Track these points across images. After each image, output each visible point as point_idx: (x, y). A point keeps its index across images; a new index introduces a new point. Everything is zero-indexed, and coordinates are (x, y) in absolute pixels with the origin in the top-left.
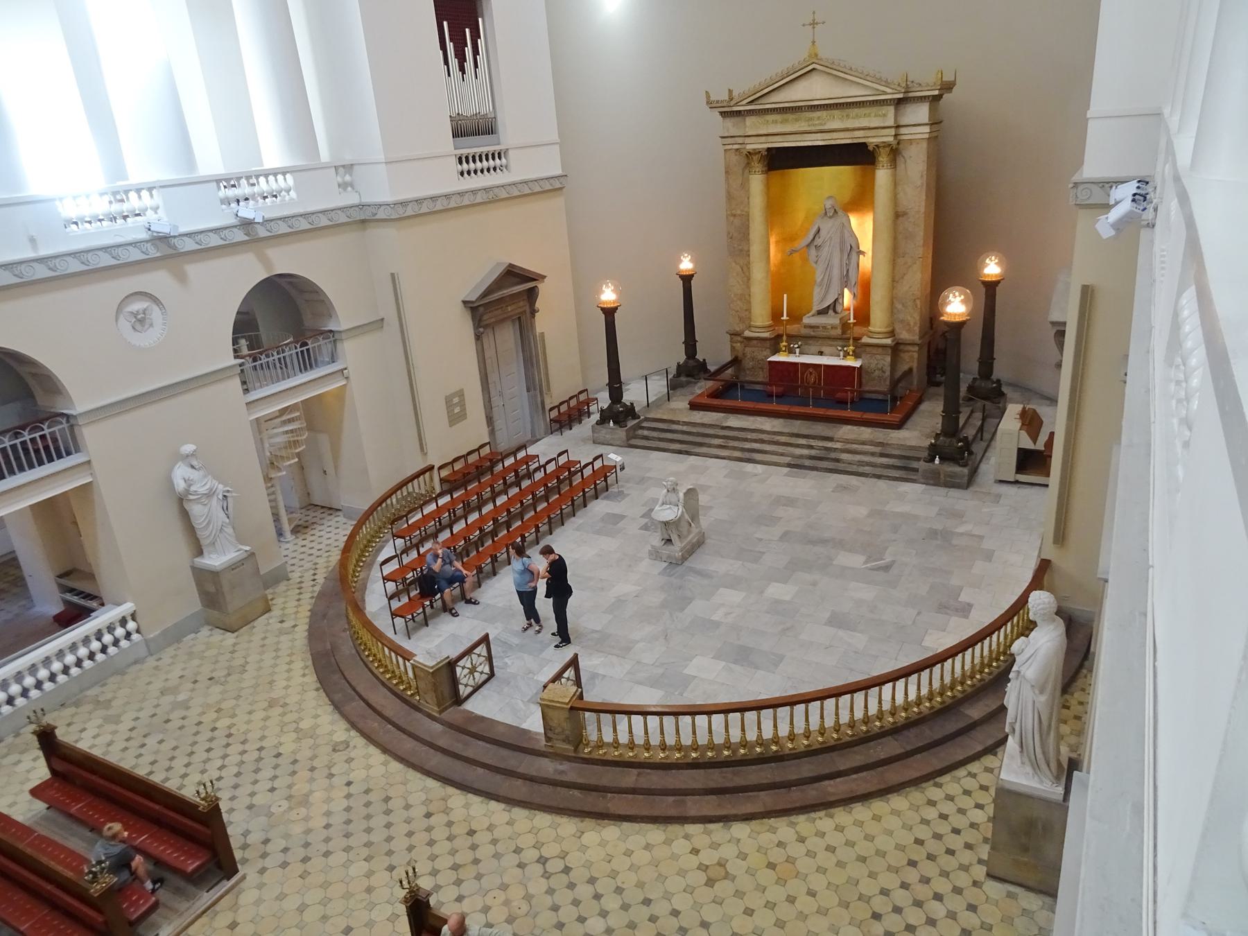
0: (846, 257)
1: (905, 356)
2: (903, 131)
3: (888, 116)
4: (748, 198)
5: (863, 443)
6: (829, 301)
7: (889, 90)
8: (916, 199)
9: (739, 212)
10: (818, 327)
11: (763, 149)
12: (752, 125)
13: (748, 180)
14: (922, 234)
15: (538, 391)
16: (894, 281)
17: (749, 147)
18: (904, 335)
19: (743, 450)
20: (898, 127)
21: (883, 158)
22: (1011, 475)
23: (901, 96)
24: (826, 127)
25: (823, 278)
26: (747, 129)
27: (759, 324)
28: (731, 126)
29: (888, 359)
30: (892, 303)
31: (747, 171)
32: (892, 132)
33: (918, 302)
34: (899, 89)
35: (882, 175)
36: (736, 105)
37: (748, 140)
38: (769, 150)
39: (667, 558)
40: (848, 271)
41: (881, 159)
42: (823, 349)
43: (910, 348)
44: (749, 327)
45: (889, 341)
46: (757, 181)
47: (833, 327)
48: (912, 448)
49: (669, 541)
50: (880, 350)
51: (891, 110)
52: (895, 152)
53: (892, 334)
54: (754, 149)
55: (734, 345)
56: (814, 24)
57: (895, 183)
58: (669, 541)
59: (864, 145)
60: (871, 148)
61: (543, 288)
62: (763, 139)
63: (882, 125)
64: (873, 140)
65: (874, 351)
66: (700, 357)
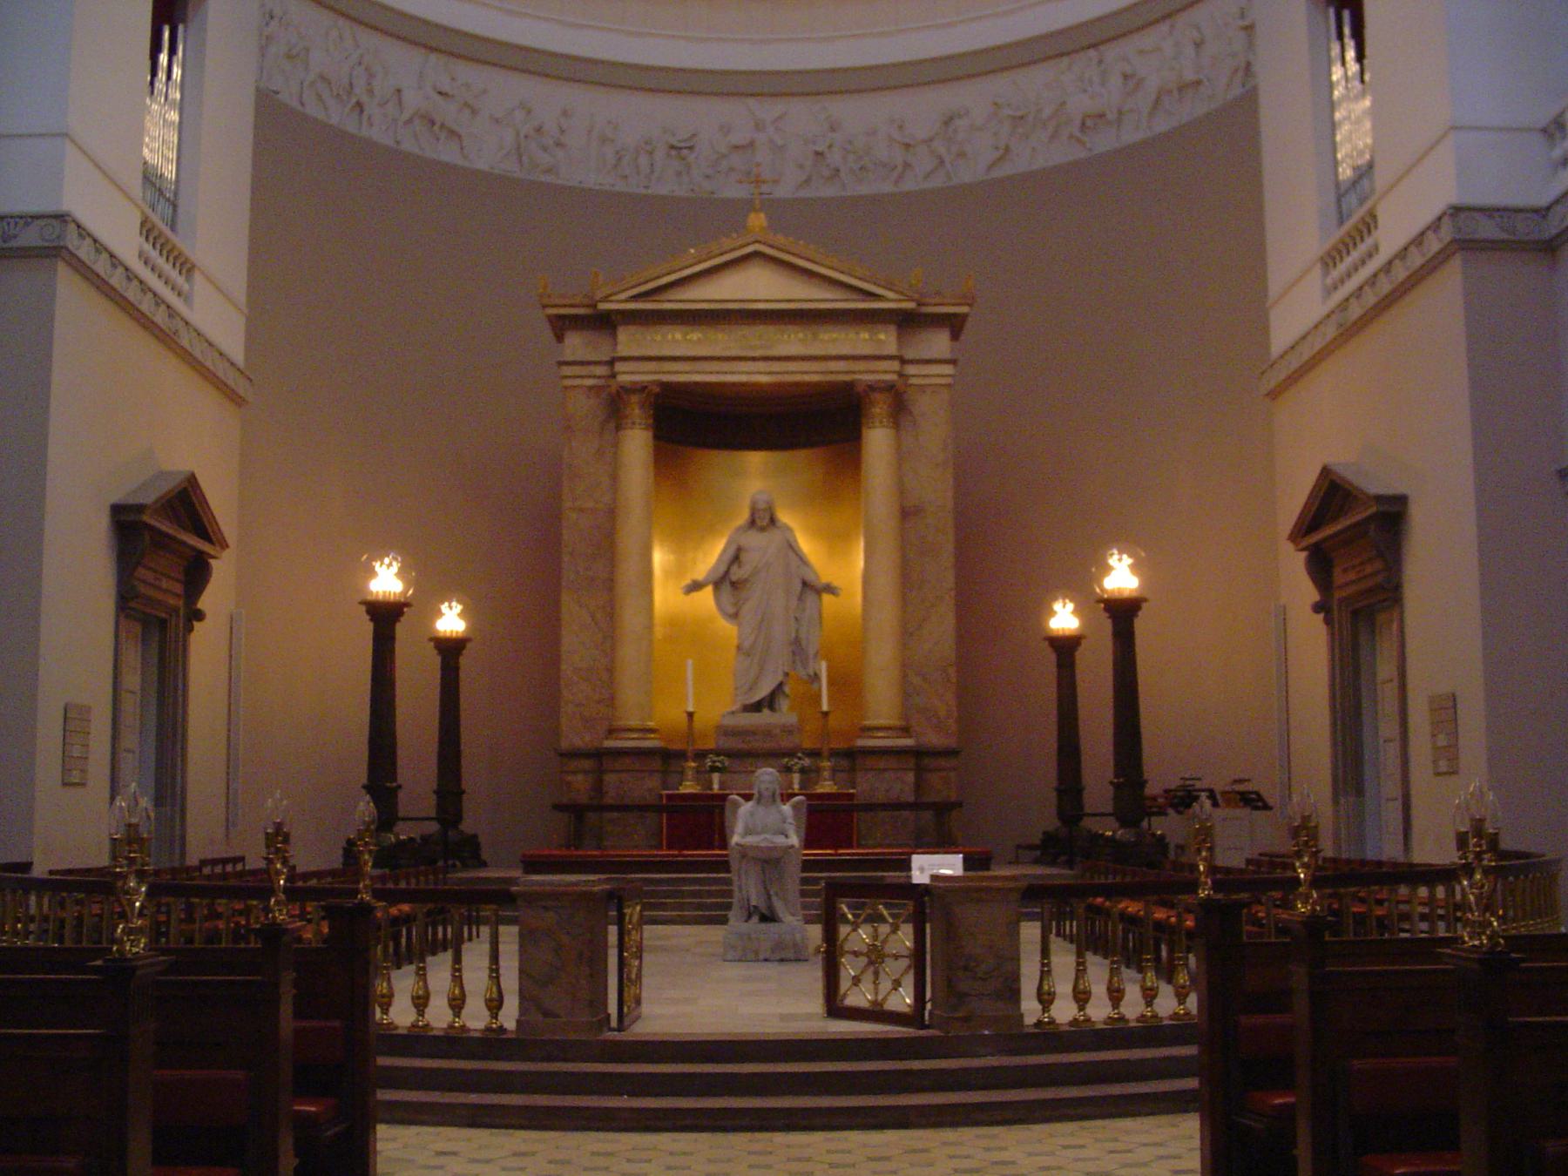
0: (794, 602)
1: (934, 779)
2: (911, 370)
3: (886, 339)
4: (615, 479)
6: (763, 692)
7: (890, 295)
8: (936, 490)
9: (591, 504)
10: (754, 733)
11: (648, 382)
12: (629, 341)
13: (616, 445)
14: (950, 547)
15: (177, 809)
16: (907, 633)
17: (624, 379)
18: (934, 739)
19: (700, 907)
20: (904, 361)
21: (879, 408)
23: (910, 305)
25: (755, 642)
26: (619, 347)
27: (634, 722)
28: (576, 344)
29: (910, 777)
30: (905, 676)
31: (612, 425)
32: (896, 365)
33: (952, 671)
34: (911, 294)
35: (877, 440)
36: (606, 299)
37: (619, 367)
38: (665, 386)
39: (773, 951)
40: (797, 631)
41: (876, 410)
43: (943, 762)
44: (611, 732)
46: (637, 444)
47: (788, 730)
51: (892, 329)
52: (899, 402)
53: (905, 731)
54: (635, 383)
55: (570, 778)
56: (757, 182)
57: (901, 456)
59: (850, 386)
60: (860, 389)
61: (222, 569)
62: (652, 366)
63: (877, 353)
64: (865, 375)
66: (467, 826)
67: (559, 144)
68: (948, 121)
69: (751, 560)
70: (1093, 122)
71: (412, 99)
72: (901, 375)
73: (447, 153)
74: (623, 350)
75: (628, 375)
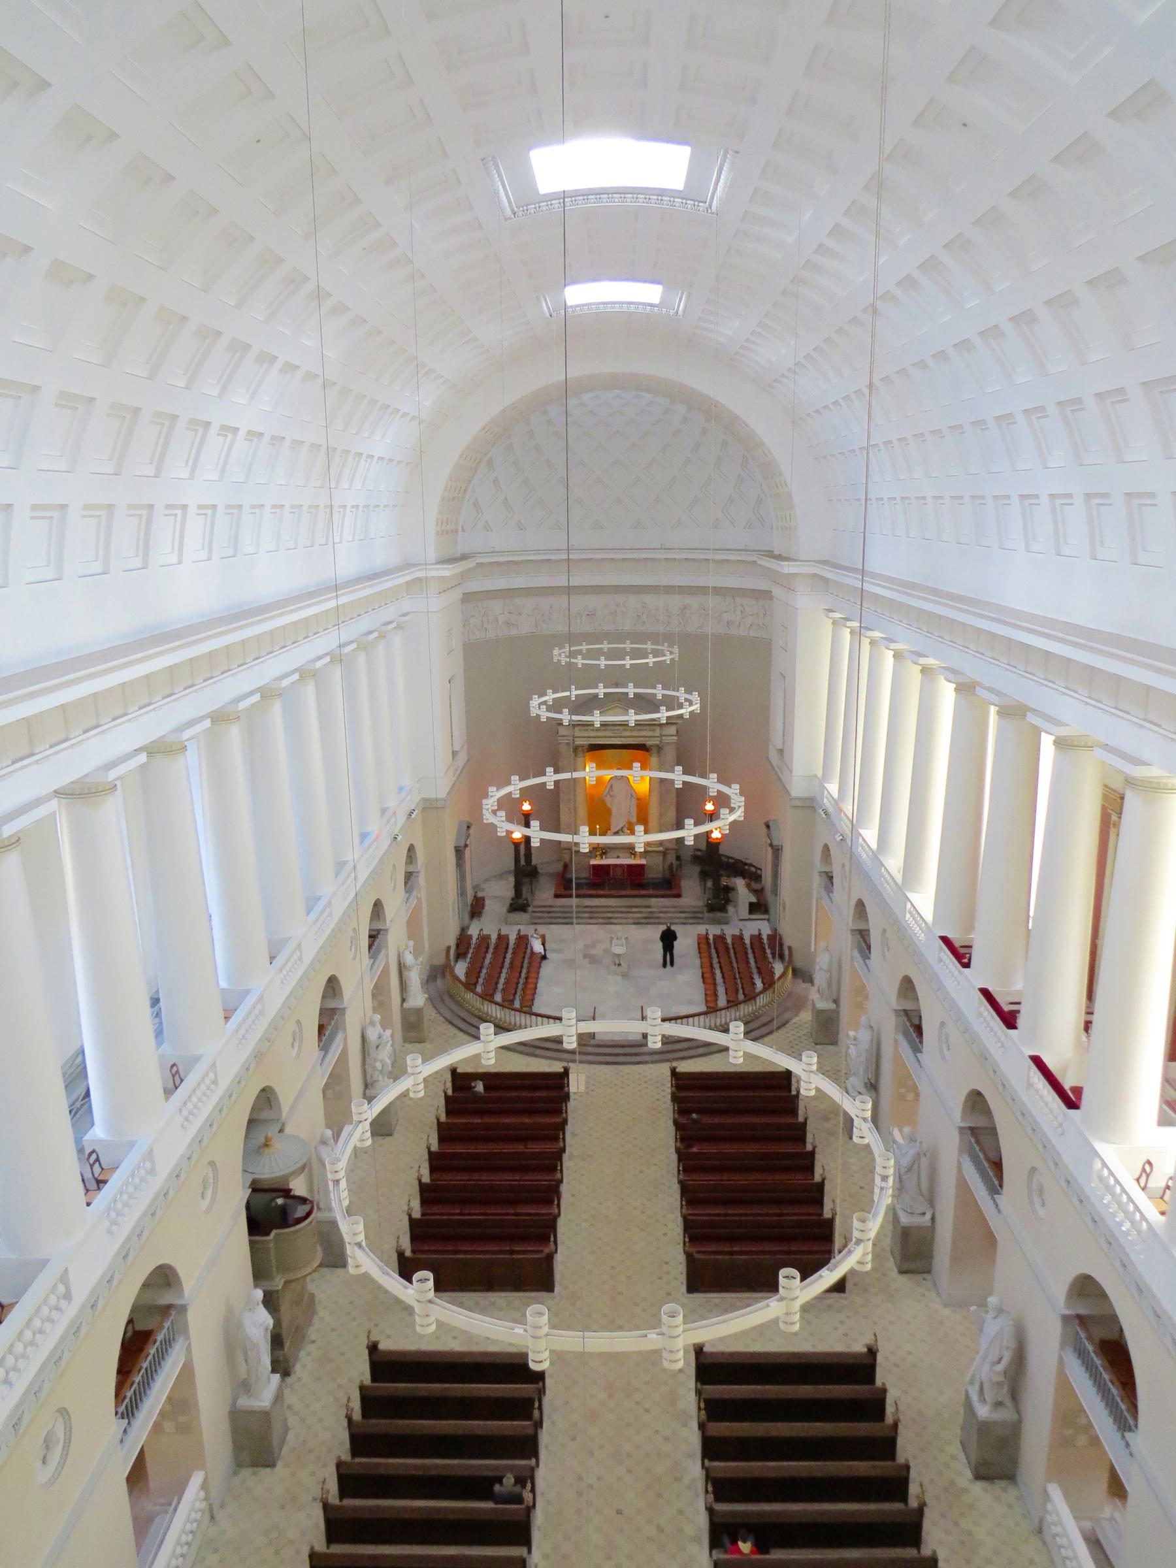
1: (669, 857)
5: (668, 907)
6: (619, 827)
17: (576, 743)
20: (661, 736)
21: (654, 751)
22: (747, 916)
24: (622, 735)
32: (659, 739)
42: (620, 855)
45: (661, 849)
48: (694, 907)
49: (619, 965)
50: (656, 854)
52: (660, 749)
58: (619, 965)
64: (649, 743)
65: (652, 854)
66: (534, 863)
67: (550, 619)
68: (685, 608)
69: (615, 788)
70: (729, 624)
71: (501, 619)
72: (660, 742)
73: (514, 632)
74: (577, 735)
75: (579, 742)
